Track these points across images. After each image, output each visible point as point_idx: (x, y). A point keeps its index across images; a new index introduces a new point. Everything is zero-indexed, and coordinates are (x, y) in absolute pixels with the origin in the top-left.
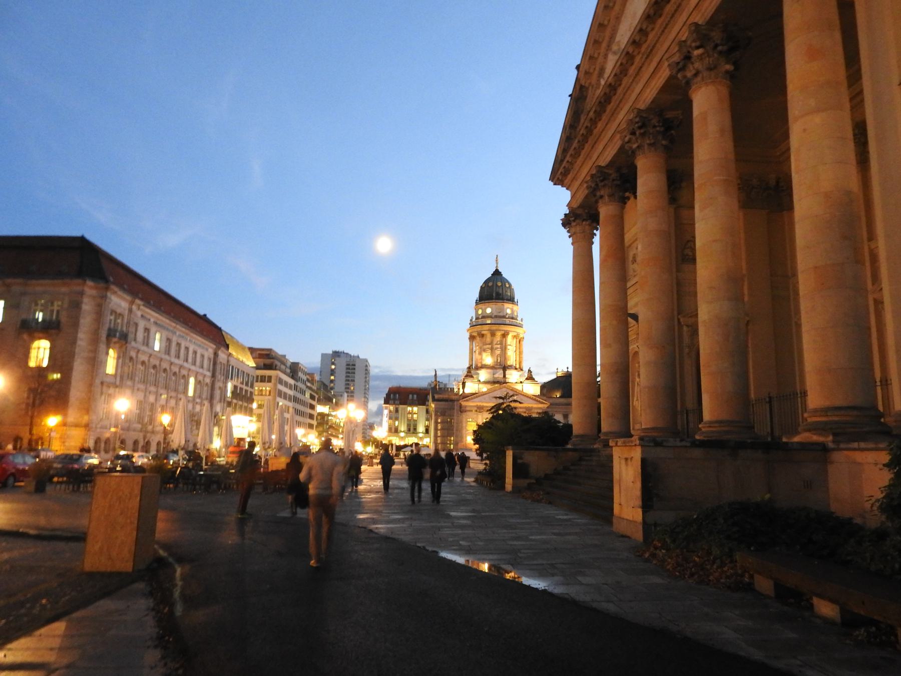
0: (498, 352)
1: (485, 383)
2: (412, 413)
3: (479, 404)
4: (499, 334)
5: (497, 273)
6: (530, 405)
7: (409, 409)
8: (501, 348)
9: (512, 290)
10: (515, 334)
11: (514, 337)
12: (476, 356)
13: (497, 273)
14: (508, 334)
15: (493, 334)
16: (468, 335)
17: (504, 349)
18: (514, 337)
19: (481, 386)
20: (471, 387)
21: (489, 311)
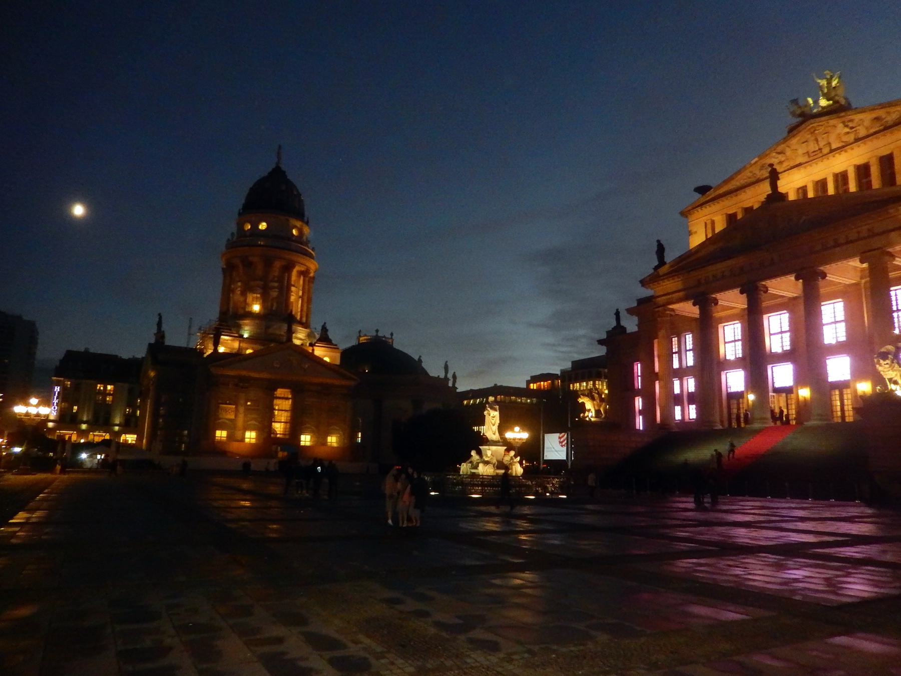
0: (274, 294)
1: (251, 340)
2: (105, 393)
3: (244, 373)
4: (278, 264)
5: (278, 174)
6: (328, 381)
7: (100, 387)
8: (281, 288)
9: (301, 202)
10: (303, 269)
11: (304, 273)
12: (237, 297)
13: (278, 174)
14: (294, 267)
15: (268, 263)
16: (221, 264)
17: (285, 291)
18: (301, 273)
19: (243, 345)
20: (227, 345)
21: (263, 226)
